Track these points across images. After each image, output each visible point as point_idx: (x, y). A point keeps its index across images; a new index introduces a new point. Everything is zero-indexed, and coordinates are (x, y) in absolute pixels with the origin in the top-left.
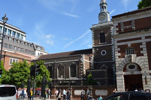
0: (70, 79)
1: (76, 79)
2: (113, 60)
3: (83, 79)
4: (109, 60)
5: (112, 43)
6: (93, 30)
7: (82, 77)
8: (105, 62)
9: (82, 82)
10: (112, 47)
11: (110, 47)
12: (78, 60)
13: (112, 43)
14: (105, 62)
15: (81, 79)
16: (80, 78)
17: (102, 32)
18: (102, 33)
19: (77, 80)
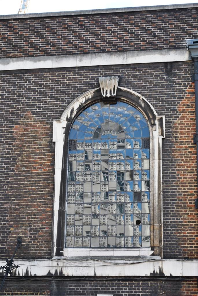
0: (70, 271)
1: (144, 270)
19: (158, 277)
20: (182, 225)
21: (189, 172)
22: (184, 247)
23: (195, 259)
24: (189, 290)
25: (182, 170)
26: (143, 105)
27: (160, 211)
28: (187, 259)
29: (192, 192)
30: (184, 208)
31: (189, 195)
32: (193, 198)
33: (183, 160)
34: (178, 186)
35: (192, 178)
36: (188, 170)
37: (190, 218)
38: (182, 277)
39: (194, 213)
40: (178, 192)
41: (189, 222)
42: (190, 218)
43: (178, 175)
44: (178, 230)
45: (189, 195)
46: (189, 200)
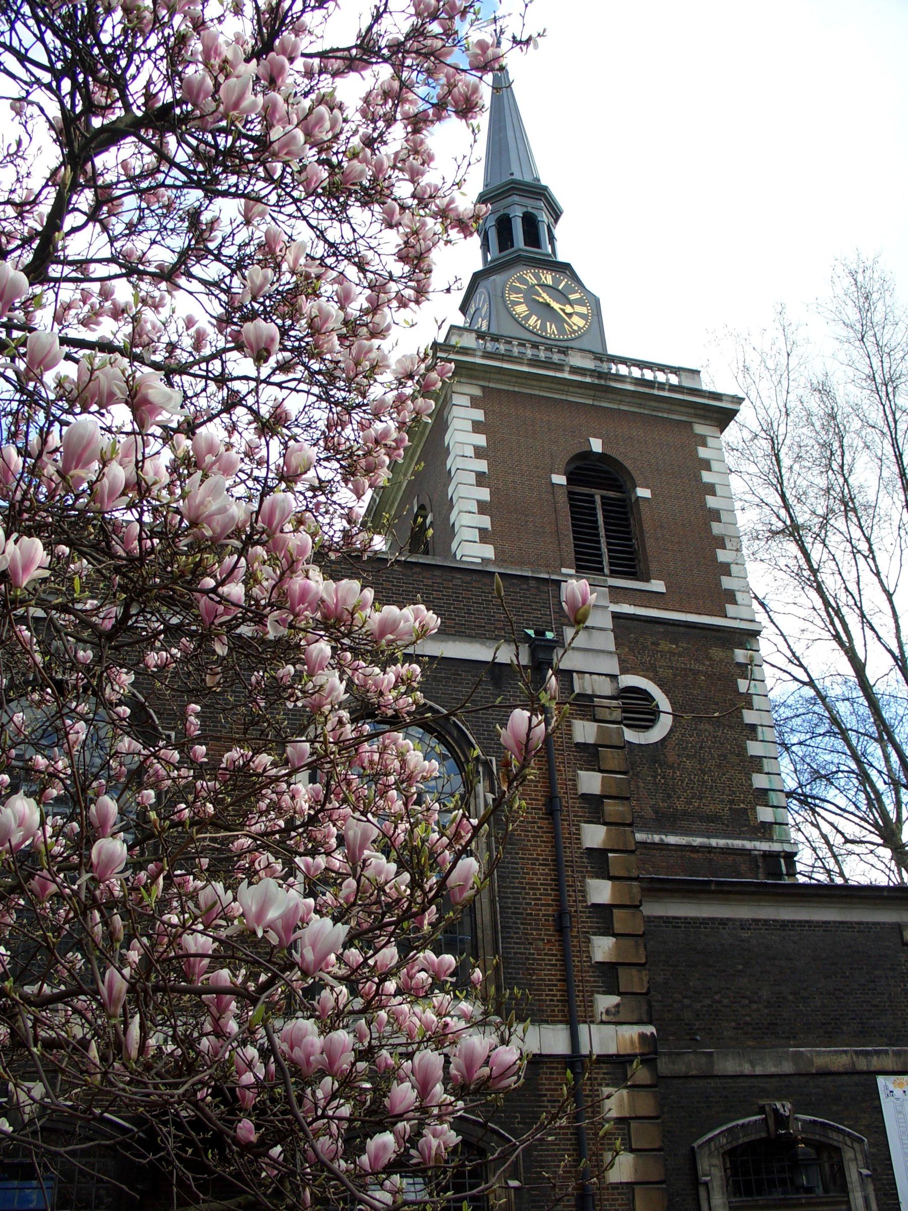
2: (766, 830)
3: (631, 1032)
4: (711, 823)
5: (730, 609)
6: (477, 392)
7: (605, 1002)
8: (672, 839)
9: (615, 1103)
10: (740, 655)
11: (717, 653)
12: (505, 655)
13: (730, 609)
14: (672, 839)
15: (602, 1039)
16: (572, 1016)
17: (597, 445)
18: (589, 454)
20: (533, 959)
21: (540, 865)
22: (539, 1000)
23: (561, 1022)
24: (552, 1079)
25: (528, 859)
26: (455, 734)
27: (495, 932)
28: (547, 1022)
29: (549, 900)
30: (536, 930)
31: (543, 905)
32: (550, 910)
33: (529, 841)
34: (524, 888)
35: (546, 874)
36: (537, 859)
37: (547, 947)
38: (541, 1055)
39: (553, 938)
40: (524, 898)
41: (546, 954)
42: (547, 947)
43: (522, 869)
44: (528, 969)
45: (543, 905)
46: (544, 915)
